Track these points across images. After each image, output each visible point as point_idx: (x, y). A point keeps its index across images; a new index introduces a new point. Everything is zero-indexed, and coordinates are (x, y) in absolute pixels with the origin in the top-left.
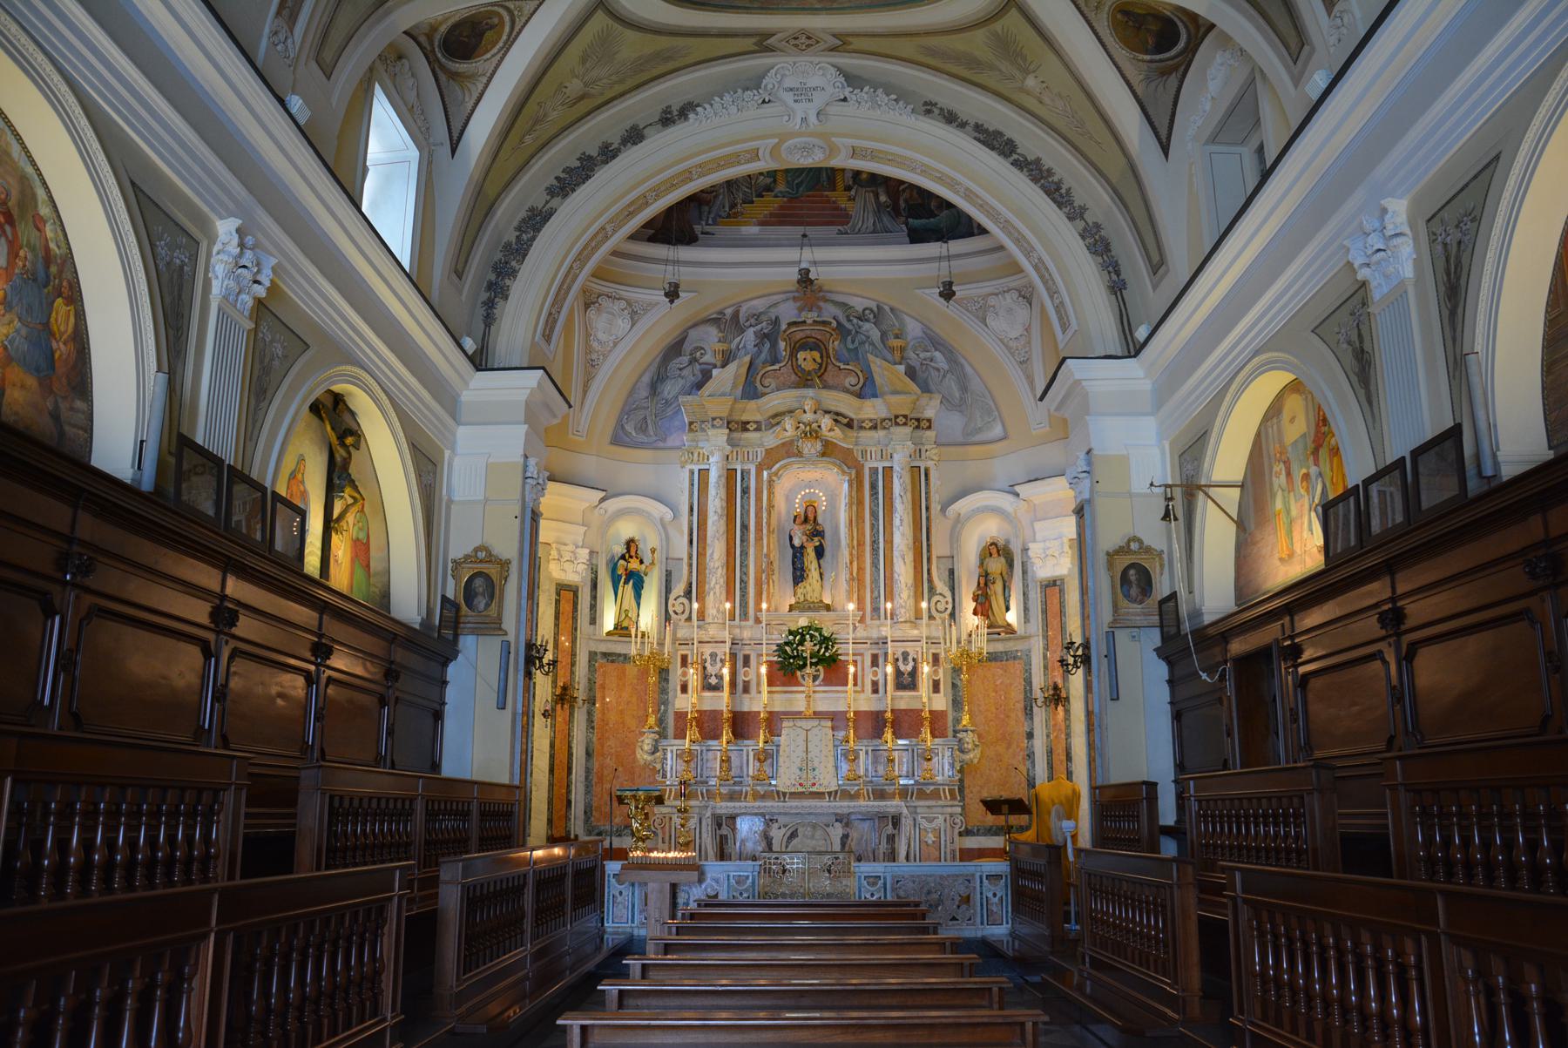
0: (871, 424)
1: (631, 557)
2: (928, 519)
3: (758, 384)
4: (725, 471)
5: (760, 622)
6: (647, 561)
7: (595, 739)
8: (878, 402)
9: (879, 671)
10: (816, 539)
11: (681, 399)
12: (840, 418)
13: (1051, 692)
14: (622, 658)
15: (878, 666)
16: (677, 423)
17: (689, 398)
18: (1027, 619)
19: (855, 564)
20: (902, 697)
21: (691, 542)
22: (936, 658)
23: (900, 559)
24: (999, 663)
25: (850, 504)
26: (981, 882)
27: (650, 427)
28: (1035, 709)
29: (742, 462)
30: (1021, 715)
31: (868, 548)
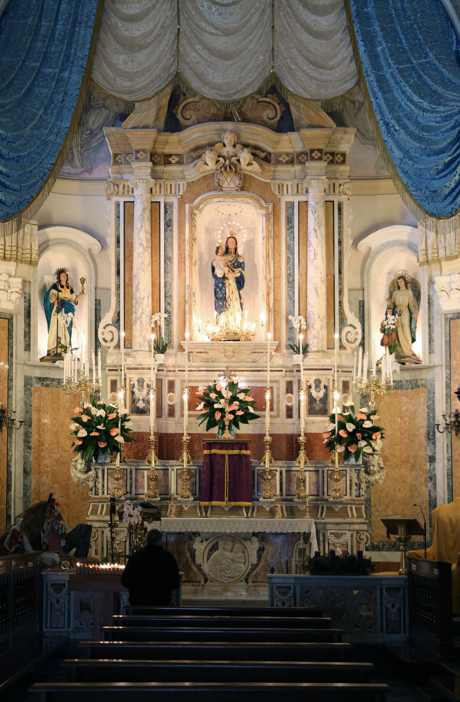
0: (287, 159)
1: (62, 287)
2: (340, 253)
3: (179, 117)
4: (149, 205)
5: (184, 350)
6: (77, 291)
7: (31, 458)
8: (293, 136)
9: (294, 397)
10: (237, 270)
11: (106, 130)
12: (258, 152)
13: (453, 419)
14: (55, 383)
15: (292, 393)
16: (102, 155)
17: (114, 129)
18: (431, 351)
19: (272, 296)
20: (314, 422)
21: (118, 273)
22: (346, 386)
23: (314, 292)
24: (404, 391)
25: (267, 238)
26: (381, 594)
27: (76, 159)
28: (437, 434)
29: (165, 195)
30: (423, 439)
31: (284, 281)
